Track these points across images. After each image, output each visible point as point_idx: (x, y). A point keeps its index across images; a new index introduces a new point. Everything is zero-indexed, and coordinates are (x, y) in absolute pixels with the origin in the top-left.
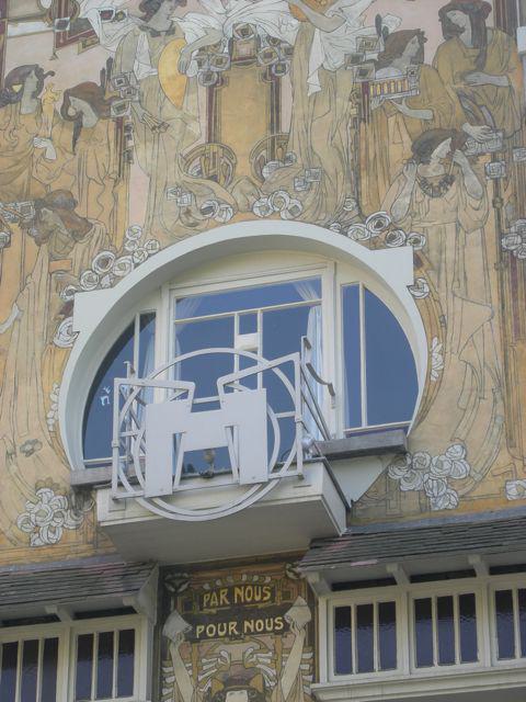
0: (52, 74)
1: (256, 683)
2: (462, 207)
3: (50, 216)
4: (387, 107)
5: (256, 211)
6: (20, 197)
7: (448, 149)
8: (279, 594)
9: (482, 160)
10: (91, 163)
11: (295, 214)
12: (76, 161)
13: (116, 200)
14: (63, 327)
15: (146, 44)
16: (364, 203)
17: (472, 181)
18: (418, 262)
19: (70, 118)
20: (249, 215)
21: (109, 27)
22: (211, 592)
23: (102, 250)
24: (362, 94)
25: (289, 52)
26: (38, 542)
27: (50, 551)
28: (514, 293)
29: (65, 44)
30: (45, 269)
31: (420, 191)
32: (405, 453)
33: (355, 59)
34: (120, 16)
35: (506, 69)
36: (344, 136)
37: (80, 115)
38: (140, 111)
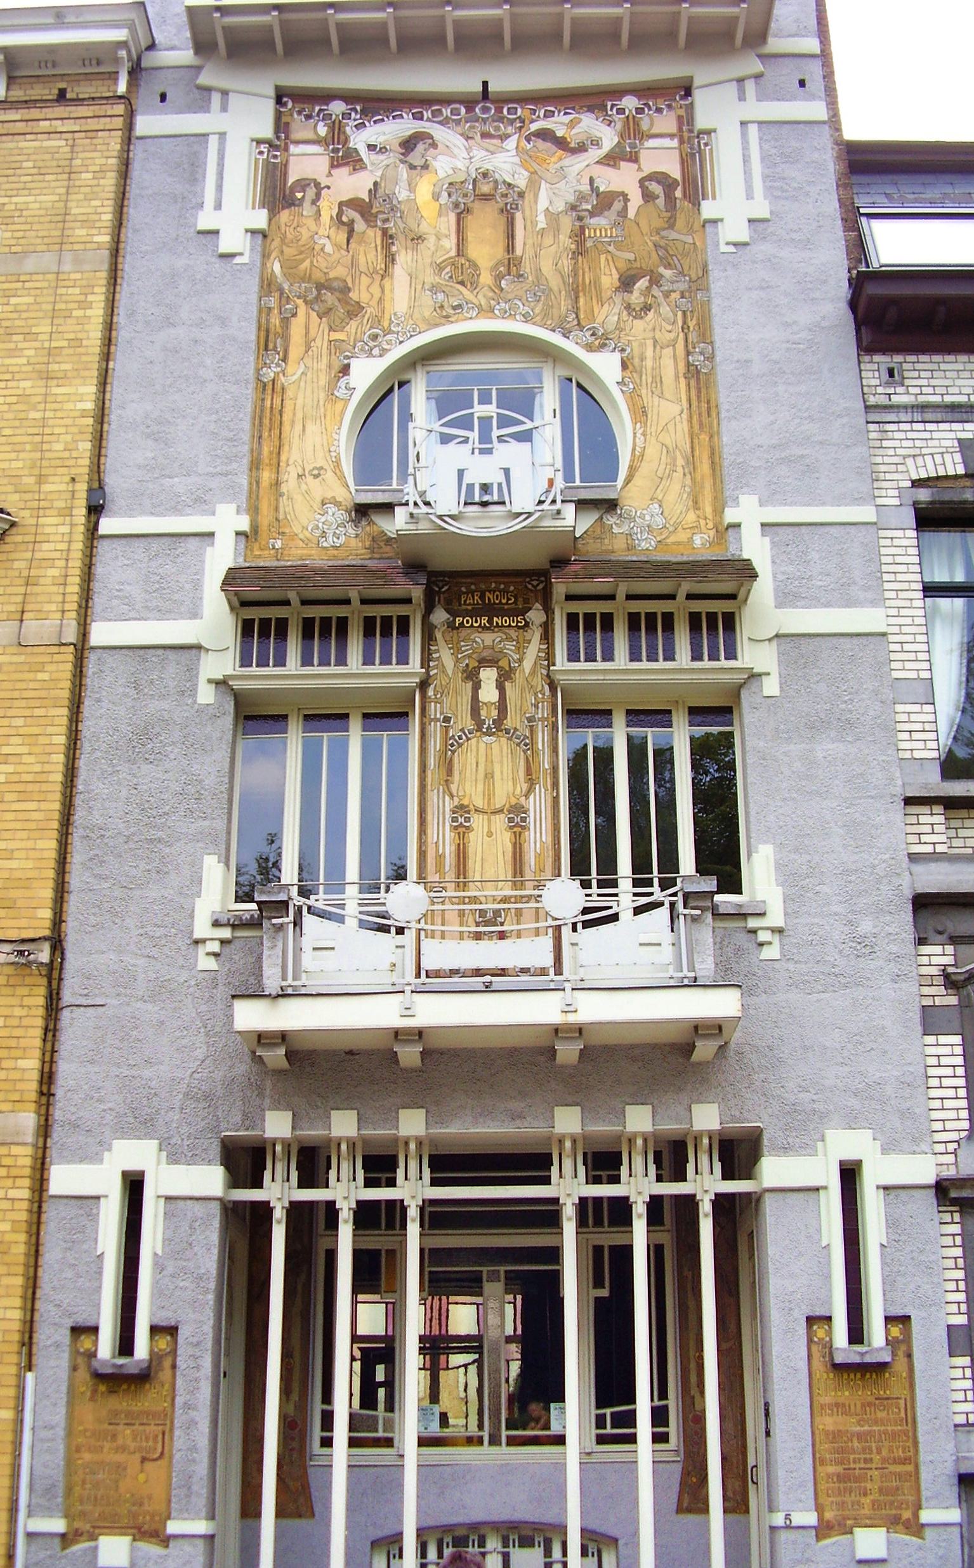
0: (329, 187)
1: (503, 663)
2: (658, 328)
3: (329, 298)
4: (600, 246)
5: (496, 312)
6: (303, 280)
7: (647, 284)
8: (521, 599)
9: (673, 295)
10: (362, 260)
11: (527, 318)
12: (349, 257)
13: (383, 291)
14: (342, 383)
15: (405, 175)
16: (582, 316)
17: (665, 310)
18: (624, 366)
19: (343, 223)
20: (490, 315)
21: (374, 157)
22: (467, 593)
23: (372, 327)
24: (579, 235)
25: (521, 195)
26: (325, 544)
27: (335, 552)
28: (699, 397)
29: (339, 166)
30: (326, 337)
31: (625, 313)
32: (616, 505)
33: (573, 208)
34: (383, 150)
35: (691, 231)
36: (565, 262)
37: (353, 221)
38: (402, 226)
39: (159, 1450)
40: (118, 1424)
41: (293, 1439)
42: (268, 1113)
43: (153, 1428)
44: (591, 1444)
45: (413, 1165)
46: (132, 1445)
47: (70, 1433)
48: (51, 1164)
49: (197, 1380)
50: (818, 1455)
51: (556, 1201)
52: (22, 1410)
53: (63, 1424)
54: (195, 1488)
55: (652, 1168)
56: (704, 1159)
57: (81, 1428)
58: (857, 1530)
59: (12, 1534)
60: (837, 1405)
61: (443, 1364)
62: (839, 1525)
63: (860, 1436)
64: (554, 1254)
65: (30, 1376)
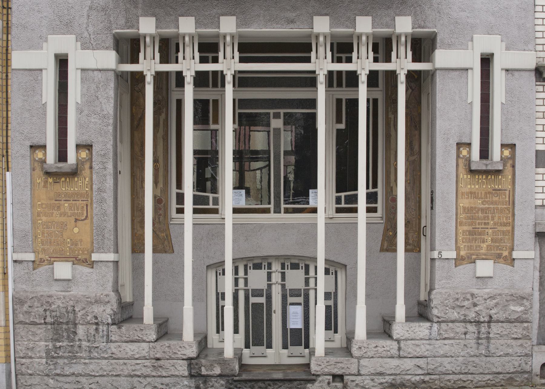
39: (85, 215)
40: (60, 200)
41: (160, 209)
42: (140, 18)
43: (80, 202)
44: (332, 213)
45: (229, 50)
46: (70, 213)
47: (33, 206)
48: (12, 50)
49: (105, 176)
50: (459, 220)
51: (314, 72)
52: (5, 193)
53: (29, 201)
54: (106, 235)
55: (371, 54)
56: (402, 49)
57: (40, 203)
58: (477, 261)
59: (5, 261)
60: (471, 193)
61: (246, 168)
62: (468, 258)
63: (482, 210)
64: (313, 103)
65: (8, 174)
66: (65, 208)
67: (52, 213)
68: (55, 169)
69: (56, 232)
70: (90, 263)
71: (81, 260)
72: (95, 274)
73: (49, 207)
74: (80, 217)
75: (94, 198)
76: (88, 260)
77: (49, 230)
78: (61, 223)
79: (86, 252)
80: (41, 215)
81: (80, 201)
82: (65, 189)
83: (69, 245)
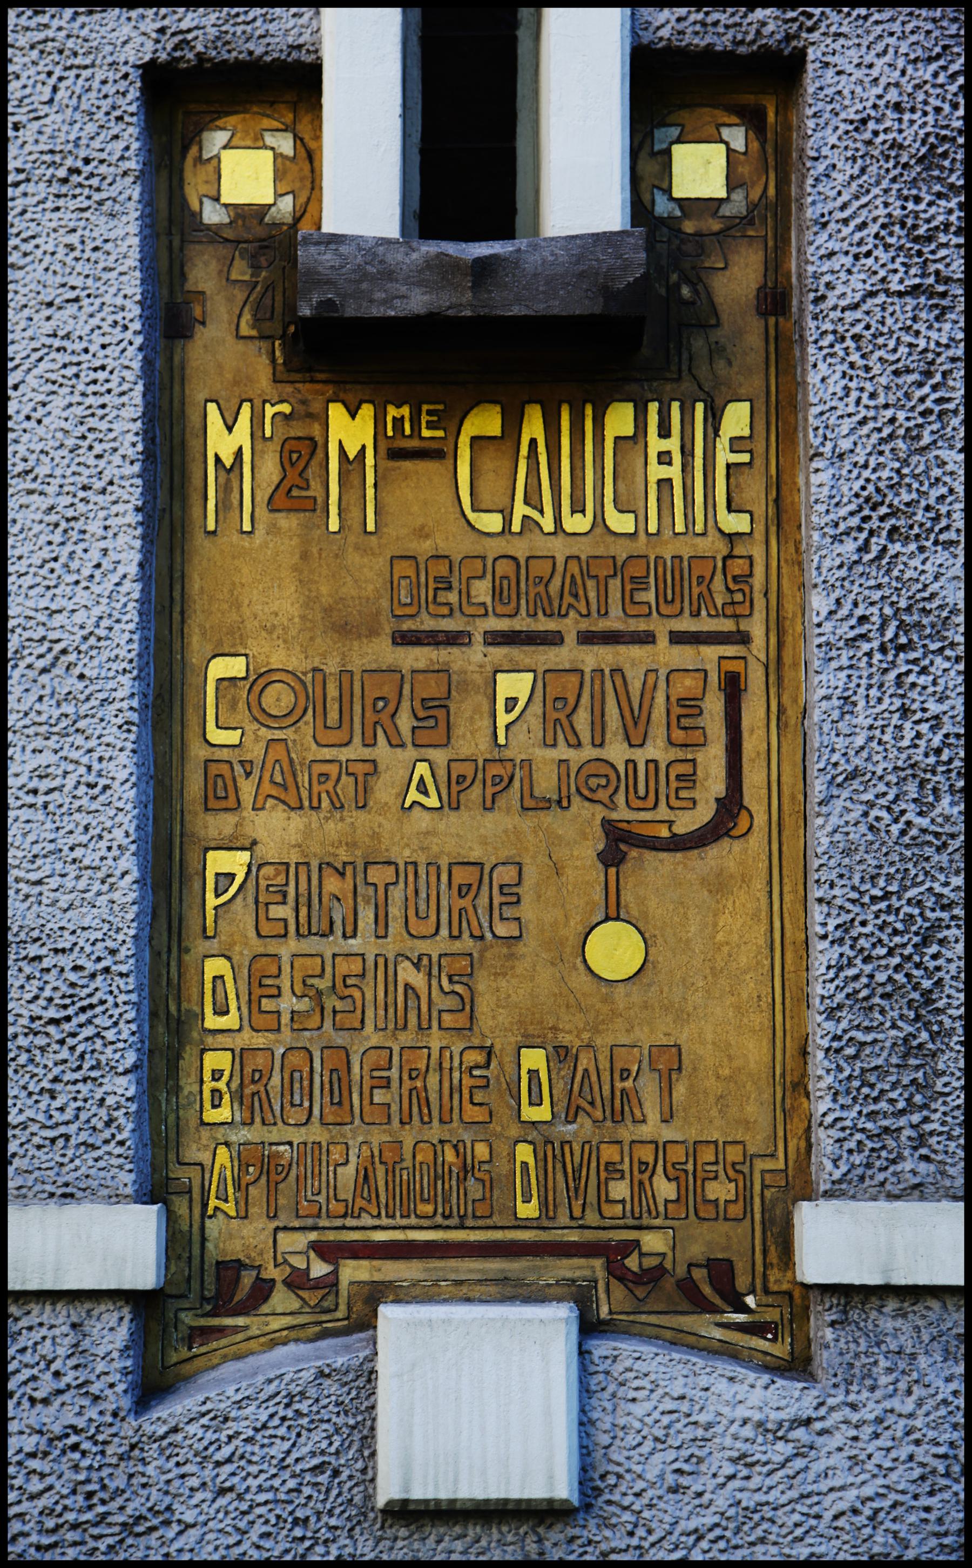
40: (454, 639)
57: (234, 667)
66: (503, 719)
67: (360, 769)
68: (419, 284)
69: (407, 973)
70: (771, 1315)
71: (669, 1284)
72: (838, 1440)
73: (333, 716)
74: (663, 812)
75: (820, 603)
76: (742, 1282)
77: (327, 947)
78: (461, 876)
79: (720, 1190)
80: (247, 789)
81: (663, 641)
82: (508, 522)
83: (542, 1113)
